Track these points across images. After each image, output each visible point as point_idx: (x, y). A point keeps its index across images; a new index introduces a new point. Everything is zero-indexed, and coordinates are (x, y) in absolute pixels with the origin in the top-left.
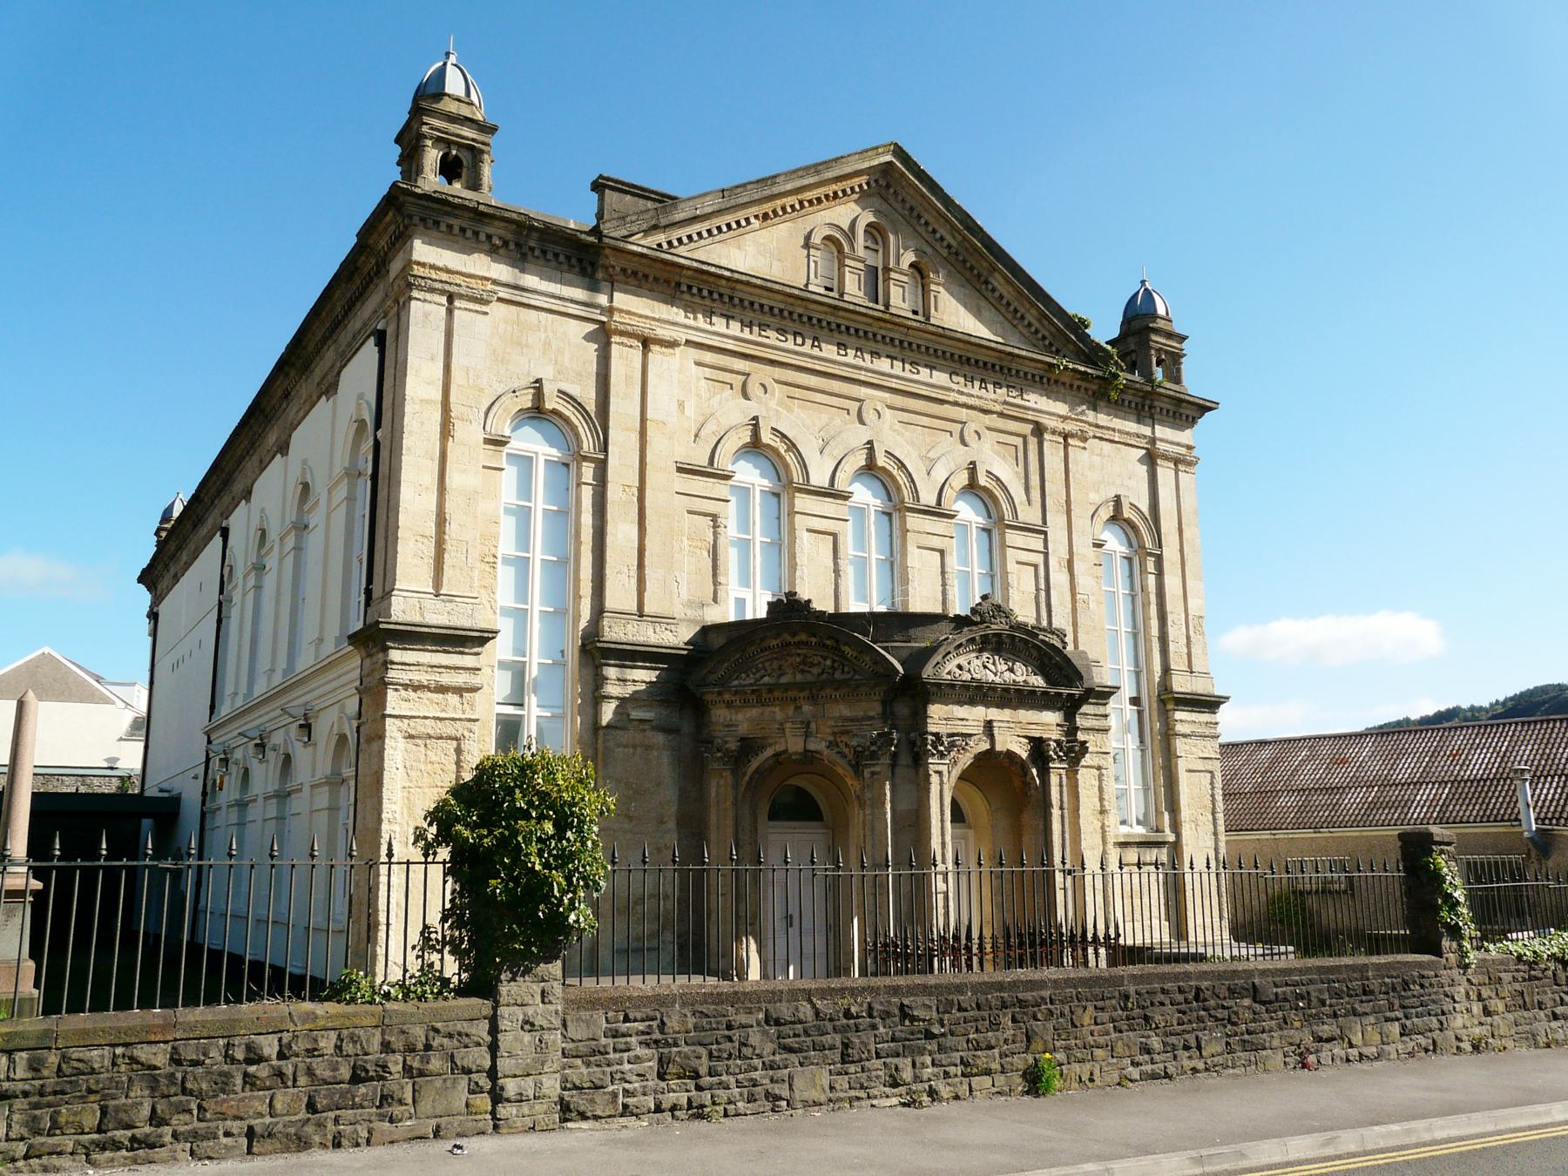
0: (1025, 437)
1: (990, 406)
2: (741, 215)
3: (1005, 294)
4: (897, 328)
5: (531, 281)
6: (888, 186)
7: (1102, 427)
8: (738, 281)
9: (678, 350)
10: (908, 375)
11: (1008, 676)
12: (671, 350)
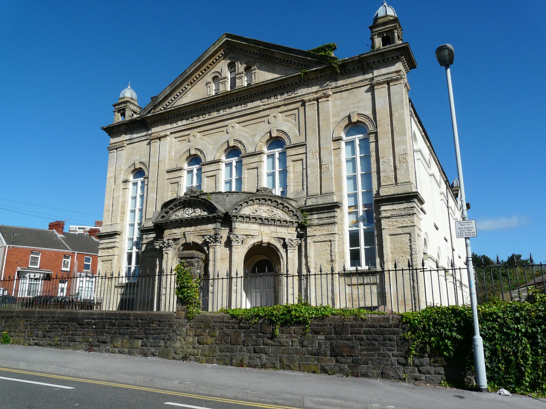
0: (298, 108)
1: (279, 104)
2: (182, 87)
3: (281, 58)
4: (232, 95)
5: (135, 136)
6: (232, 47)
7: (339, 87)
8: (179, 108)
9: (168, 137)
10: (244, 108)
11: (194, 214)
12: (166, 138)
